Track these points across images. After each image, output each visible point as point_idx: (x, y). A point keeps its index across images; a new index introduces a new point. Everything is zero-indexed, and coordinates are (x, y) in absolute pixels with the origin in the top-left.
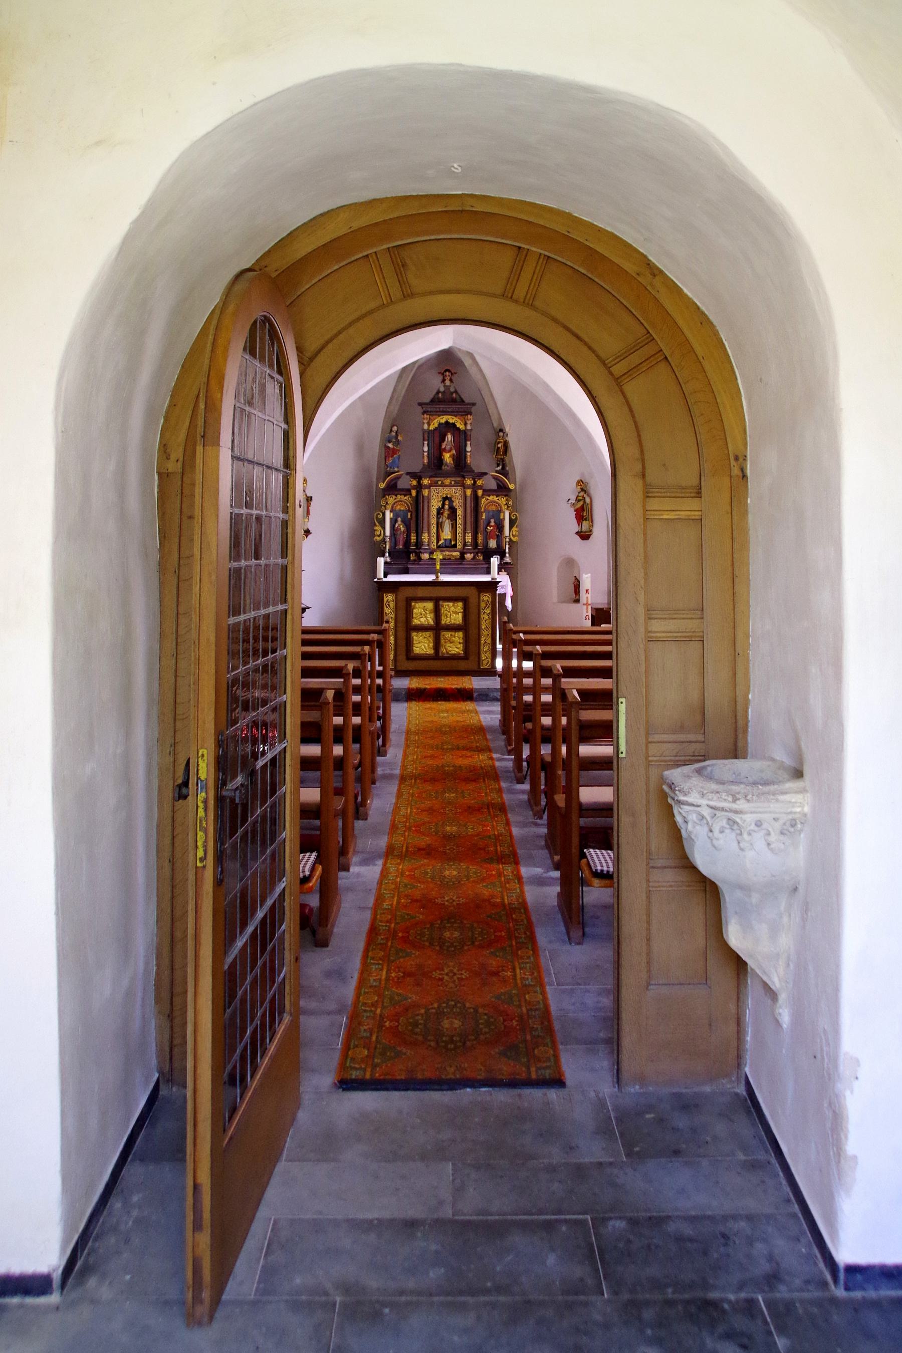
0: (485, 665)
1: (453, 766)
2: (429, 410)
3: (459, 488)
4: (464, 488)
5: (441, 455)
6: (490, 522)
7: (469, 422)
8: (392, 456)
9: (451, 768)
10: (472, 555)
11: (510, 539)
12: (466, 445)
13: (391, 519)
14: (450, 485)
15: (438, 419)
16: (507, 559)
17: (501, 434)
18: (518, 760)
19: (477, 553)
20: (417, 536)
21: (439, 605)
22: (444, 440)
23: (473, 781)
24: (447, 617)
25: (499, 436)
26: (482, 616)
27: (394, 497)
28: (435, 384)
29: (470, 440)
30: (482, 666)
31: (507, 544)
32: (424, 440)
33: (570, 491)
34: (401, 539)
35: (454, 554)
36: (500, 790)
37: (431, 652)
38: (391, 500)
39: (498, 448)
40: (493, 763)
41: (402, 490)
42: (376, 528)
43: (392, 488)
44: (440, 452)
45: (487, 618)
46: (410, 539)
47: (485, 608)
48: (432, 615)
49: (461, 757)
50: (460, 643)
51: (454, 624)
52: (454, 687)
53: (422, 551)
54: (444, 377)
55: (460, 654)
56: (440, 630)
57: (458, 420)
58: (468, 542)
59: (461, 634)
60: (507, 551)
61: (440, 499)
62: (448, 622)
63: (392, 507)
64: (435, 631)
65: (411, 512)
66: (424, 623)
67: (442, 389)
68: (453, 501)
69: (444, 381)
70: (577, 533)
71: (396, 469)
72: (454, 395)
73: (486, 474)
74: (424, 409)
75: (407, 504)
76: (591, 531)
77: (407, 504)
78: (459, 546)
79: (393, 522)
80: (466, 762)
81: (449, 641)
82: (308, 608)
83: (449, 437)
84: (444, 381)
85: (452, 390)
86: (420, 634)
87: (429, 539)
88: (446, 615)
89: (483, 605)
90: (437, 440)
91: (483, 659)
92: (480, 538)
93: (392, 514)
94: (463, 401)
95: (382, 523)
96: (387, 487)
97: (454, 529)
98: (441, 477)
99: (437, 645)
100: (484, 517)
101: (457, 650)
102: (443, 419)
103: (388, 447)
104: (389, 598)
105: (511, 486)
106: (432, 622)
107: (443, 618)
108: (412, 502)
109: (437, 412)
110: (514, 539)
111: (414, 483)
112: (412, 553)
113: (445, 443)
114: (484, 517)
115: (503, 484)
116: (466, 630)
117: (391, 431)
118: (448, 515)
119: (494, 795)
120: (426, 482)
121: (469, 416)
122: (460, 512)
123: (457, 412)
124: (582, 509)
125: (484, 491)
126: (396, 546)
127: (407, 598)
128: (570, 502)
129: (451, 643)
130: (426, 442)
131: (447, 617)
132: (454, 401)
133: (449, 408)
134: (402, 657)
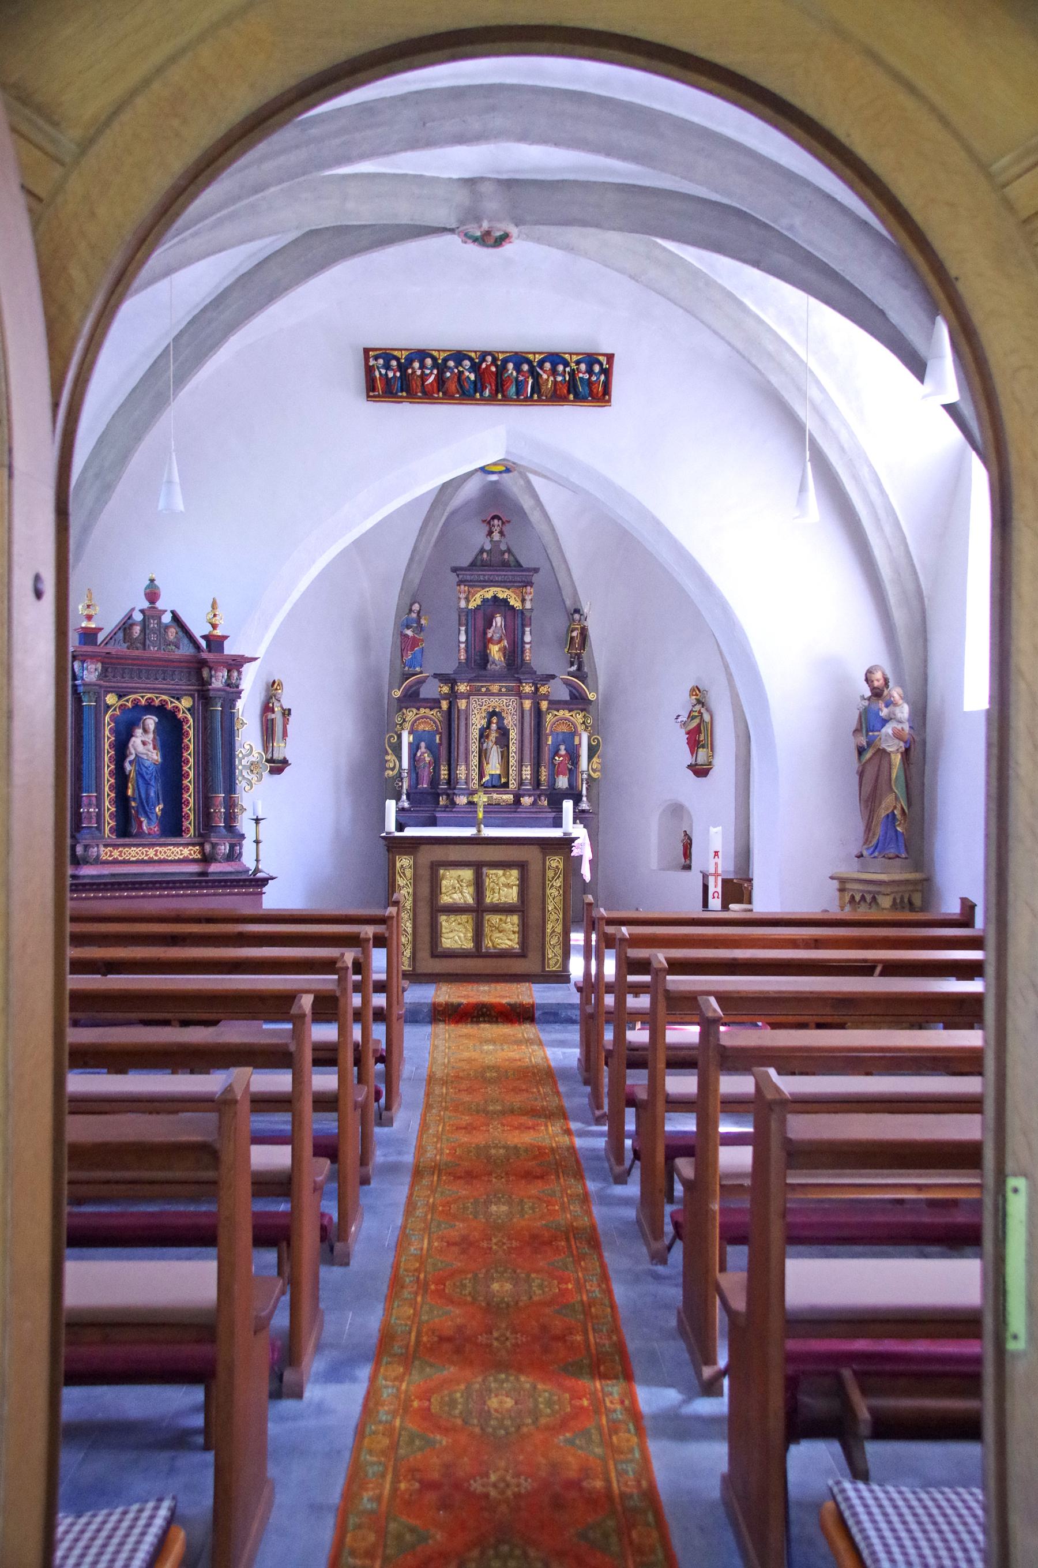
0: (553, 965)
1: (504, 1147)
2: (468, 578)
3: (513, 698)
4: (521, 698)
5: (485, 647)
6: (559, 750)
7: (528, 598)
8: (412, 649)
9: (502, 1151)
10: (532, 799)
11: (589, 775)
12: (523, 633)
13: (410, 744)
14: (499, 694)
15: (482, 592)
16: (584, 805)
17: (577, 616)
18: (616, 1135)
19: (539, 796)
20: (449, 770)
21: (482, 873)
22: (490, 625)
23: (537, 1177)
24: (494, 892)
25: (574, 620)
26: (548, 892)
27: (415, 711)
28: (477, 538)
30: (549, 967)
31: (585, 782)
32: (460, 625)
33: (681, 703)
34: (426, 773)
35: (505, 797)
36: (585, 1198)
37: (469, 945)
38: (410, 715)
39: (572, 638)
40: (572, 1143)
41: (426, 700)
42: (388, 758)
43: (412, 698)
44: (486, 642)
45: (556, 894)
46: (439, 775)
47: (553, 878)
48: (471, 889)
49: (516, 1128)
50: (514, 932)
51: (505, 903)
52: (504, 1001)
53: (456, 791)
54: (490, 528)
55: (514, 949)
56: (484, 911)
57: (513, 596)
58: (526, 779)
59: (515, 919)
60: (584, 792)
61: (484, 714)
62: (495, 901)
63: (413, 725)
64: (474, 914)
65: (440, 733)
66: (458, 901)
67: (488, 547)
68: (503, 719)
69: (490, 533)
70: (690, 767)
71: (418, 669)
72: (506, 556)
73: (553, 677)
74: (461, 576)
75: (435, 722)
76: (710, 763)
77: (435, 722)
78: (513, 785)
79: (414, 748)
80: (528, 1138)
81: (497, 928)
82: (272, 878)
83: (498, 620)
84: (490, 533)
85: (503, 547)
86: (452, 918)
87: (467, 775)
88: (493, 889)
89: (550, 874)
91: (550, 956)
92: (544, 773)
93: (411, 737)
94: (518, 565)
95: (397, 749)
96: (405, 696)
97: (505, 760)
98: (487, 681)
99: (478, 935)
100: (550, 742)
101: (510, 943)
102: (489, 593)
103: (407, 636)
104: (404, 862)
105: (591, 696)
106: (470, 900)
107: (488, 893)
108: (441, 719)
109: (481, 581)
110: (595, 775)
111: (446, 689)
112: (442, 794)
113: (493, 629)
114: (550, 742)
115: (578, 691)
116: (523, 911)
117: (411, 611)
118: (496, 738)
119: (576, 1208)
120: (462, 688)
121: (529, 588)
122: (513, 735)
123: (510, 582)
124: (697, 730)
125: (551, 702)
126: (417, 784)
127: (432, 863)
128: (679, 720)
129: (500, 932)
130: (463, 628)
131: (494, 892)
132: (505, 565)
133: (497, 575)
134: (424, 954)
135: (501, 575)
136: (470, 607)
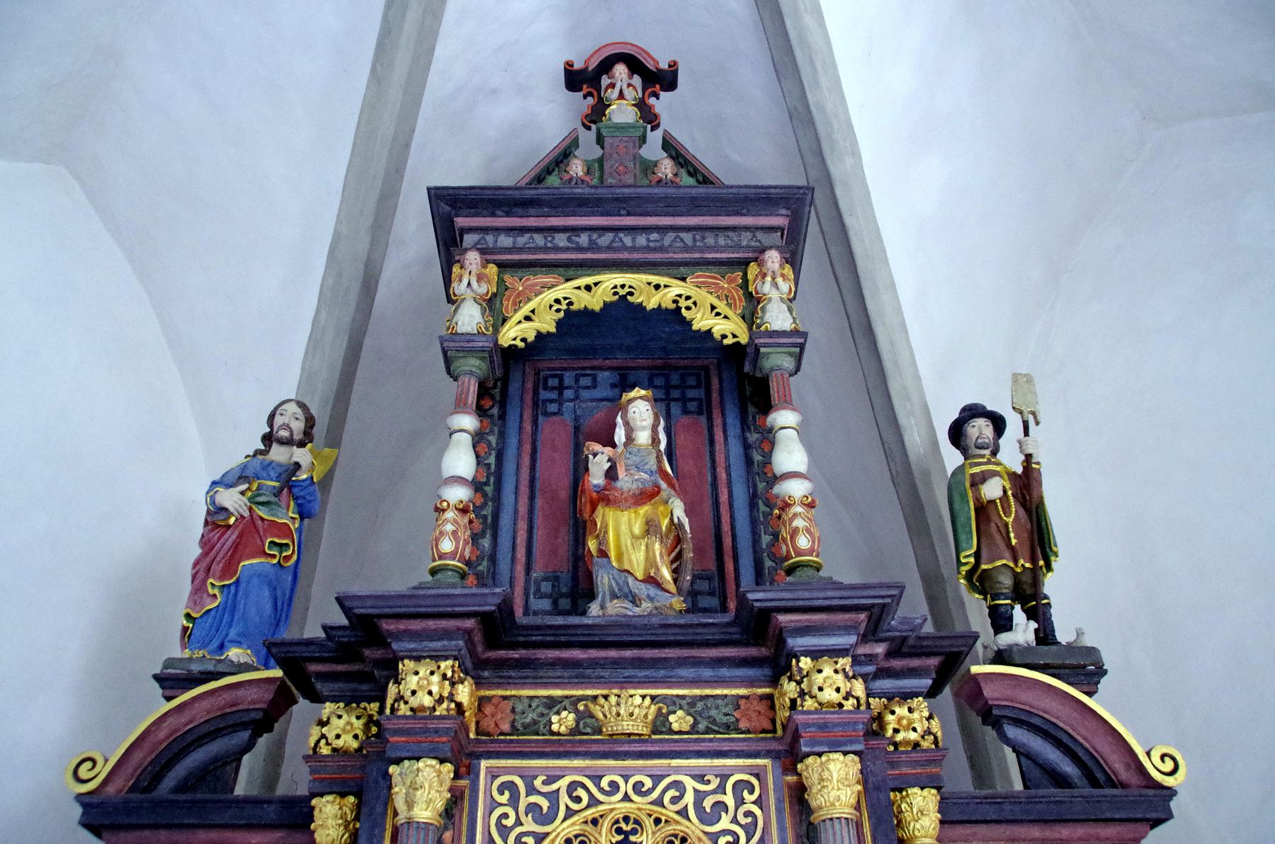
5: (580, 528)
15: (565, 290)
29: (788, 404)
98: (578, 672)
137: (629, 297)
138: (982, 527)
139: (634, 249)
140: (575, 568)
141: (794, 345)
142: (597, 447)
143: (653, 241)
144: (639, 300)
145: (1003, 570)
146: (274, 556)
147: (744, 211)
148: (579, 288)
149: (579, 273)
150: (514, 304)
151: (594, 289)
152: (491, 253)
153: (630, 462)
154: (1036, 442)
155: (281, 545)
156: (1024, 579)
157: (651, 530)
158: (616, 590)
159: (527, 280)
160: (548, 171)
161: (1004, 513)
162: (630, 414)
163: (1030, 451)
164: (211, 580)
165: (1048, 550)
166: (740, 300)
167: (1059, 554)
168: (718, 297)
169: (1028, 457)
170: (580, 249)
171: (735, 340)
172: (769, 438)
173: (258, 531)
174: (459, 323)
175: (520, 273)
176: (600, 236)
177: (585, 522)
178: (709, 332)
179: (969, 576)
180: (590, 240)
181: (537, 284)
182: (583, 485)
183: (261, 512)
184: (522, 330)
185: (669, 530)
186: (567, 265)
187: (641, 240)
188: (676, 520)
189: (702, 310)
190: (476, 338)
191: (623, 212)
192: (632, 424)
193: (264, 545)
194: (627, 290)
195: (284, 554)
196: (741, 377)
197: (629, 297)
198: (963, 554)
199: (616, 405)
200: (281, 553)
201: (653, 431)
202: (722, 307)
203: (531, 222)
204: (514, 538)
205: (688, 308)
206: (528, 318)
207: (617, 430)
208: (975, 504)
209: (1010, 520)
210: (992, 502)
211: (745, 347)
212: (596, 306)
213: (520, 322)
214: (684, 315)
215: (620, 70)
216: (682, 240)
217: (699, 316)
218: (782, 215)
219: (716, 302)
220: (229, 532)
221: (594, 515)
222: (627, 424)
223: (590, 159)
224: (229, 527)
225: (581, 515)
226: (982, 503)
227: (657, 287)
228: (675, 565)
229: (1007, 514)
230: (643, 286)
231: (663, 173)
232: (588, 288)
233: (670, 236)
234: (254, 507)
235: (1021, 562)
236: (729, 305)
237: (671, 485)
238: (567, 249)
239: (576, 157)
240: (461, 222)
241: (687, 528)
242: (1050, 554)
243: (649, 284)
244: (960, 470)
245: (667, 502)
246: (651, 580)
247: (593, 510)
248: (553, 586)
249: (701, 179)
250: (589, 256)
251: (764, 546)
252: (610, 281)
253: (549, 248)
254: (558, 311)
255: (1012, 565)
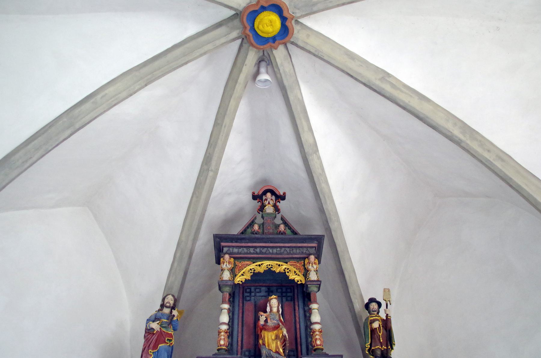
2: (236, 250)
5: (257, 337)
15: (253, 266)
57: (293, 269)
90: (249, 318)
135: (276, 247)
136: (236, 282)
137: (271, 269)
138: (373, 336)
139: (273, 254)
140: (255, 348)
141: (317, 284)
142: (262, 313)
143: (278, 251)
144: (274, 270)
145: (378, 349)
146: (168, 343)
147: (305, 242)
148: (257, 265)
149: (257, 261)
150: (239, 270)
151: (261, 266)
152: (231, 255)
153: (271, 318)
154: (389, 310)
155: (170, 340)
156: (385, 352)
157: (277, 337)
158: (268, 355)
159: (242, 263)
160: (248, 227)
161: (379, 332)
162: (271, 303)
163: (387, 313)
164: (150, 350)
165: (392, 343)
166: (303, 270)
167: (395, 344)
168: (297, 269)
169: (387, 315)
170: (257, 253)
171: (301, 282)
172: (310, 311)
173: (163, 335)
174: (224, 277)
175: (240, 261)
176: (263, 249)
177: (258, 335)
178: (294, 280)
179: (369, 350)
180: (260, 250)
181: (245, 264)
182: (258, 324)
183: (164, 330)
184: (241, 278)
185: (282, 337)
186: (254, 258)
187: (275, 251)
188: (284, 335)
189: (292, 273)
190: (228, 281)
191: (270, 242)
192: (272, 306)
193: (165, 340)
194: (271, 266)
195: (171, 343)
196: (303, 292)
197: (271, 269)
198: (366, 344)
199: (268, 301)
200: (170, 342)
201: (278, 308)
202: (298, 272)
203: (243, 244)
204: (238, 339)
205: (288, 272)
206: (242, 275)
207: (268, 307)
208: (370, 329)
209: (381, 334)
210: (376, 329)
211: (304, 284)
212: (262, 271)
213: (240, 276)
214: (287, 274)
215: (269, 194)
216: (286, 251)
217: (291, 275)
218: (315, 243)
219: (296, 270)
220: (154, 336)
221: (261, 333)
222: (270, 306)
223: (260, 223)
224: (154, 334)
225: (257, 333)
226: (373, 329)
227: (279, 265)
228: (284, 348)
229: (380, 332)
230: (275, 265)
231: (281, 229)
232: (259, 265)
233: (283, 249)
234: (161, 328)
235: (383, 347)
236: (299, 271)
237: (283, 324)
238: (253, 253)
239: (256, 223)
240: (223, 244)
241: (287, 337)
242: (392, 344)
243: (277, 264)
244: (367, 319)
245: (281, 329)
246: (277, 352)
247: (261, 331)
248: (249, 353)
249: (292, 231)
250: (260, 256)
251: (309, 342)
252: (266, 263)
253: (248, 253)
254: (251, 273)
255: (380, 348)
